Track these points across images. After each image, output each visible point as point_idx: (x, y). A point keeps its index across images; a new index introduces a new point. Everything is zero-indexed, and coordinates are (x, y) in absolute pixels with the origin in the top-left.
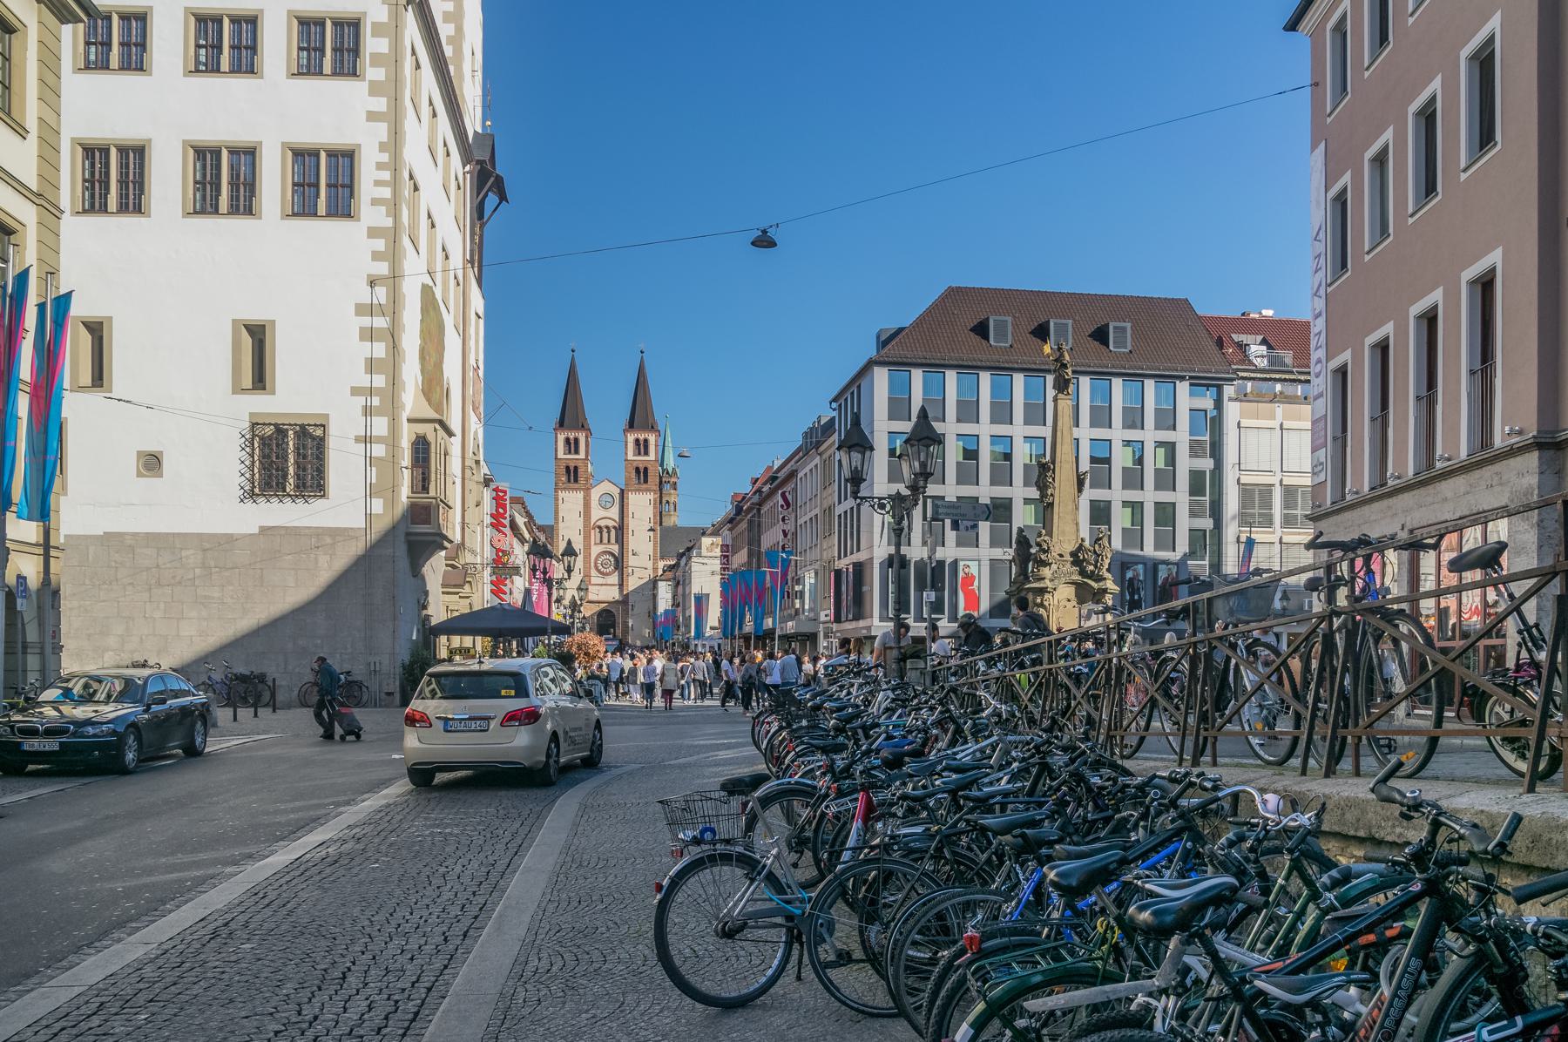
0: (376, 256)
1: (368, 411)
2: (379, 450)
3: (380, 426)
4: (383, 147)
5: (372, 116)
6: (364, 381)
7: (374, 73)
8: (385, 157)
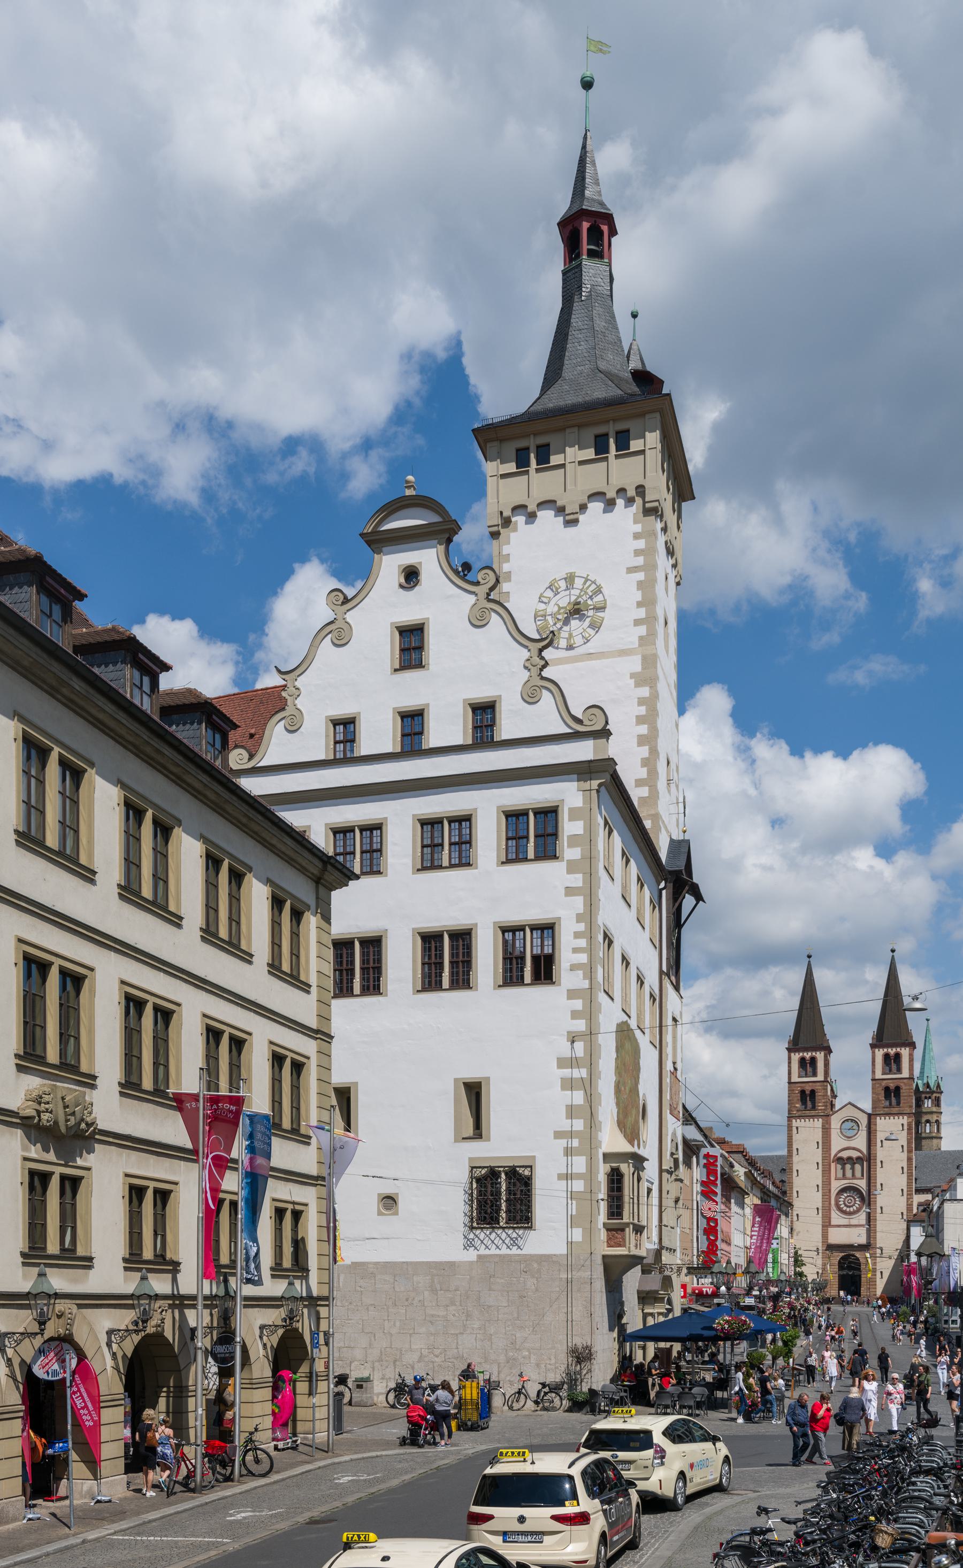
0: (575, 1015)
1: (569, 1152)
2: (578, 1186)
3: (580, 1164)
4: (579, 918)
5: (570, 891)
6: (565, 1125)
7: (570, 853)
8: (581, 927)
